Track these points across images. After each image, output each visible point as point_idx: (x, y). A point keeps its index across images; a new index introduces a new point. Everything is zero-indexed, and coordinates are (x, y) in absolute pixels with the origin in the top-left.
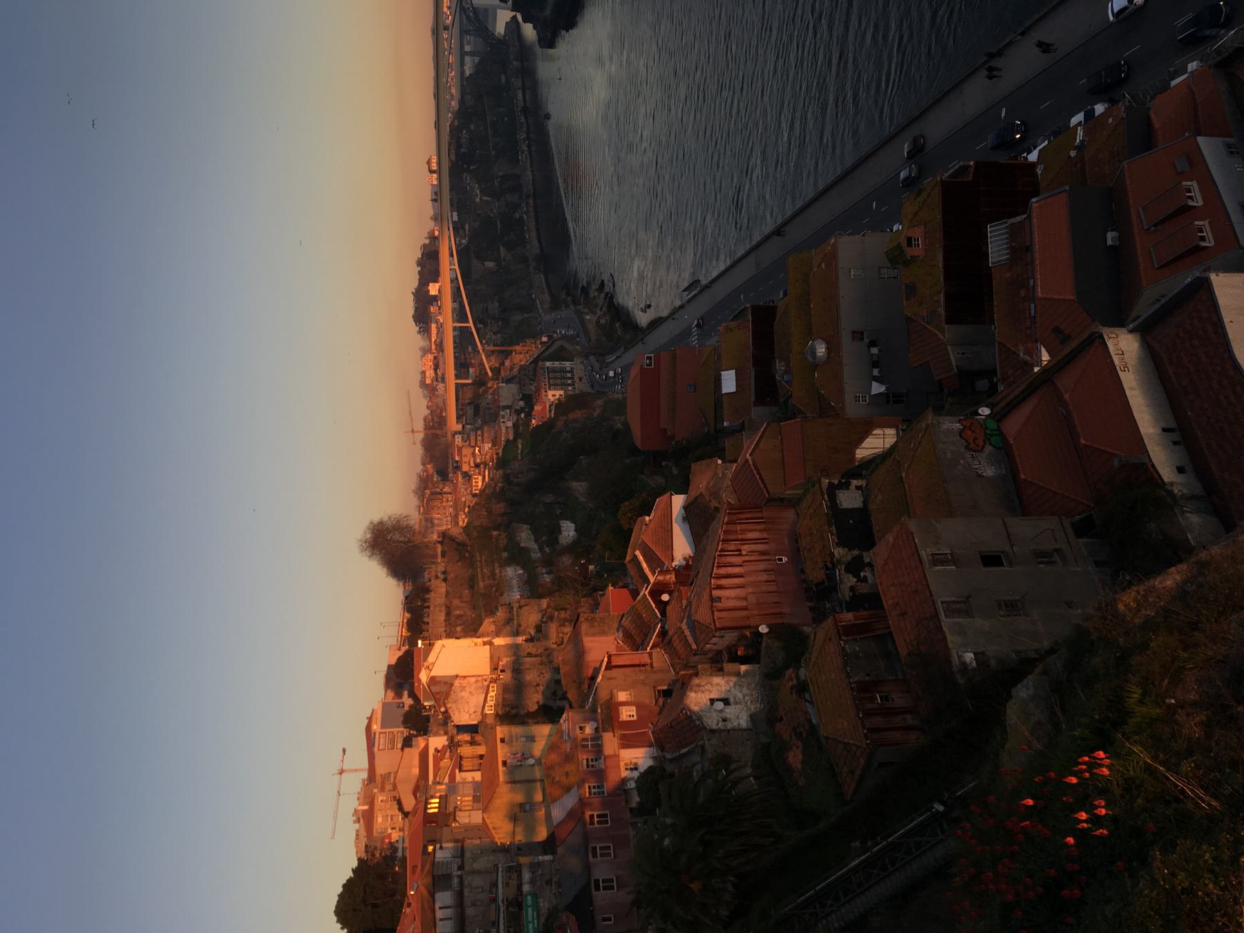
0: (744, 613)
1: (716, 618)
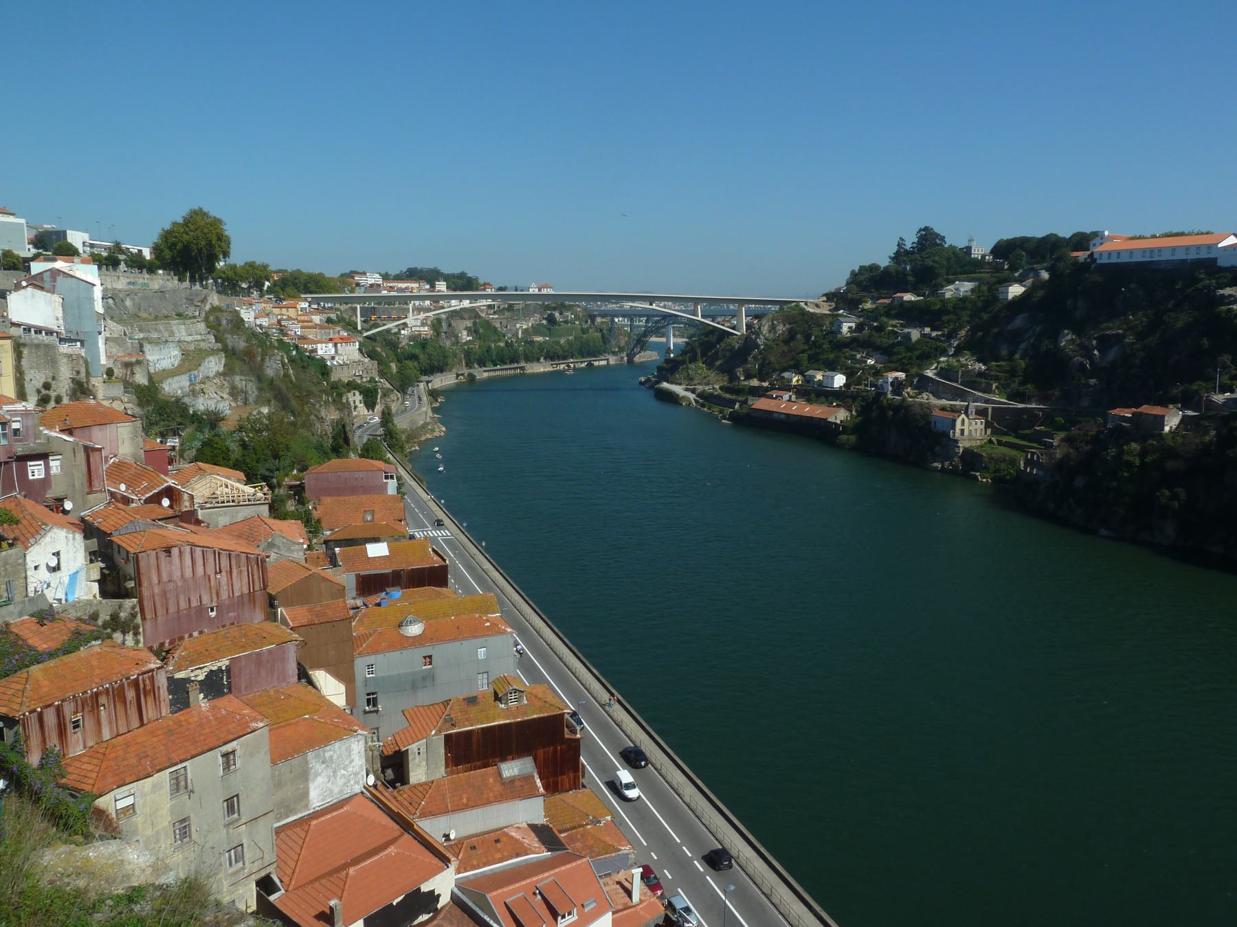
0: (155, 580)
1: (148, 552)
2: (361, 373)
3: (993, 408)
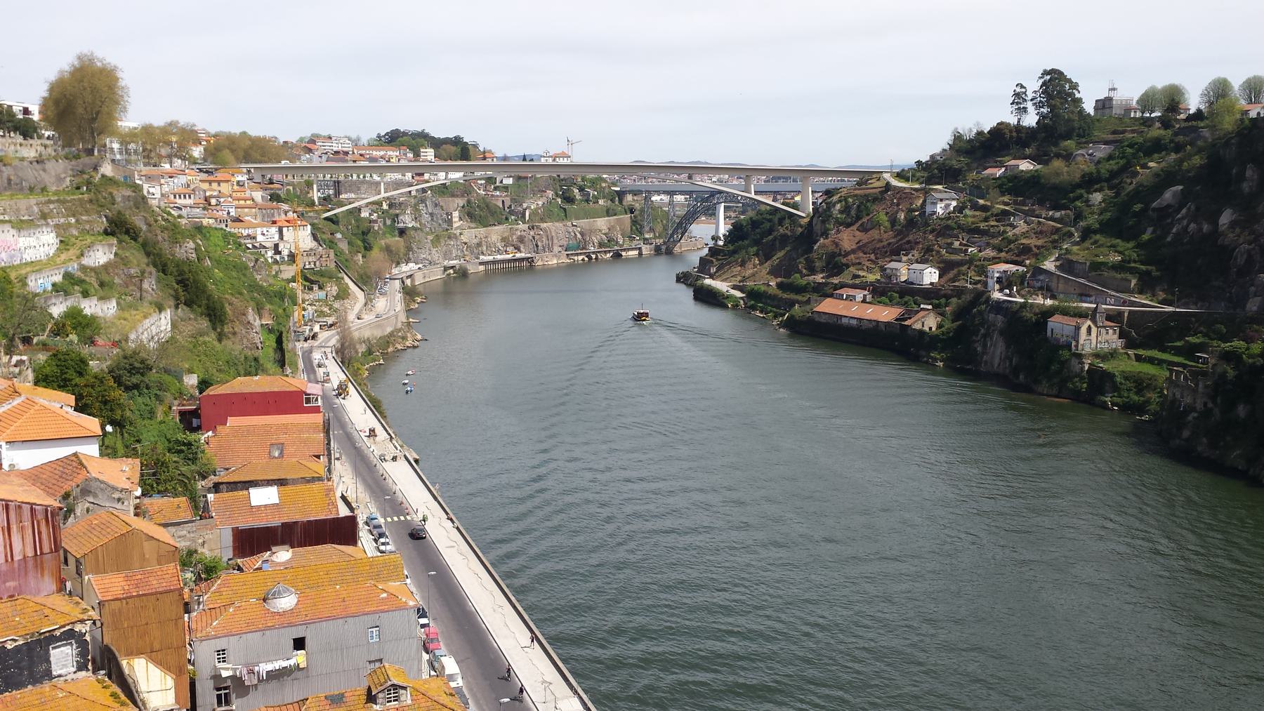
2: (313, 266)
3: (1130, 312)
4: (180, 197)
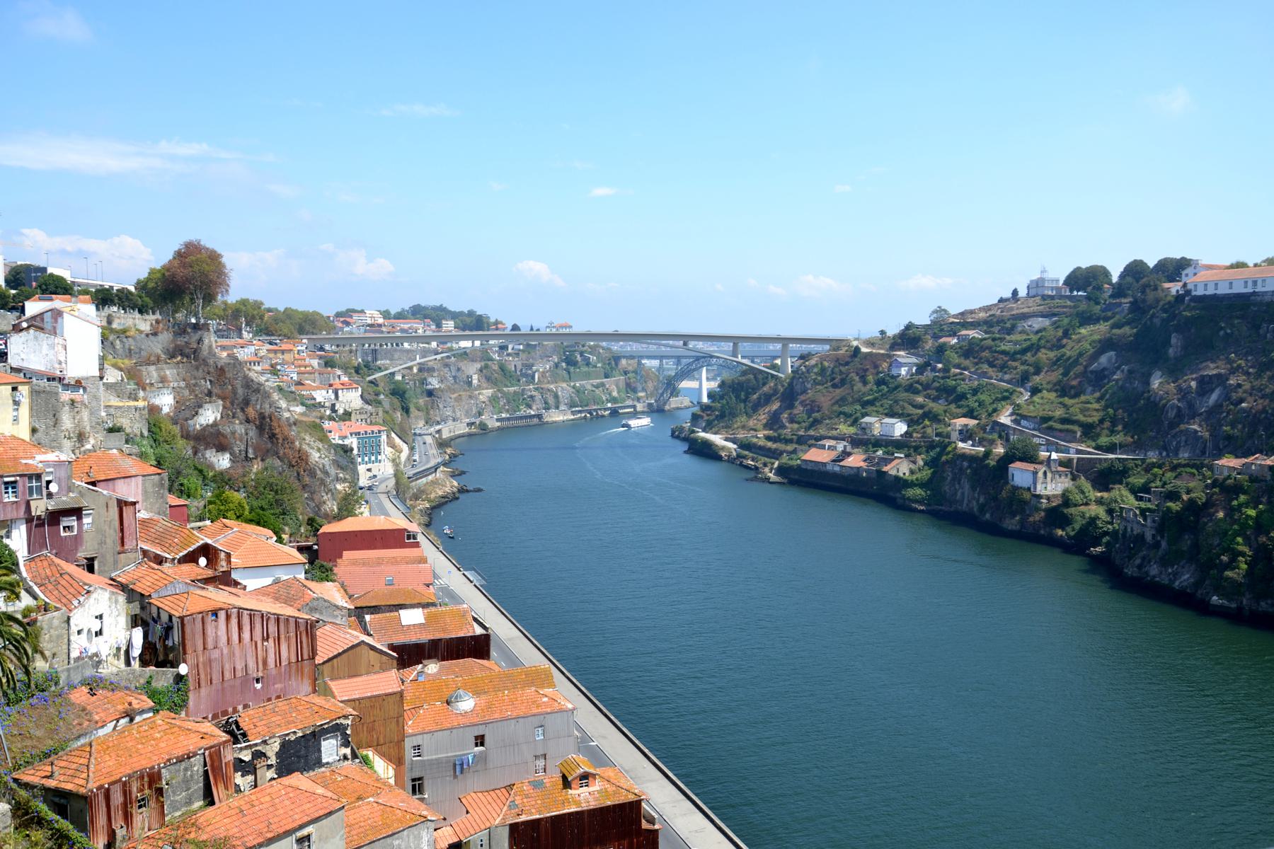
0: (200, 647)
3: (1078, 459)
4: (255, 365)
